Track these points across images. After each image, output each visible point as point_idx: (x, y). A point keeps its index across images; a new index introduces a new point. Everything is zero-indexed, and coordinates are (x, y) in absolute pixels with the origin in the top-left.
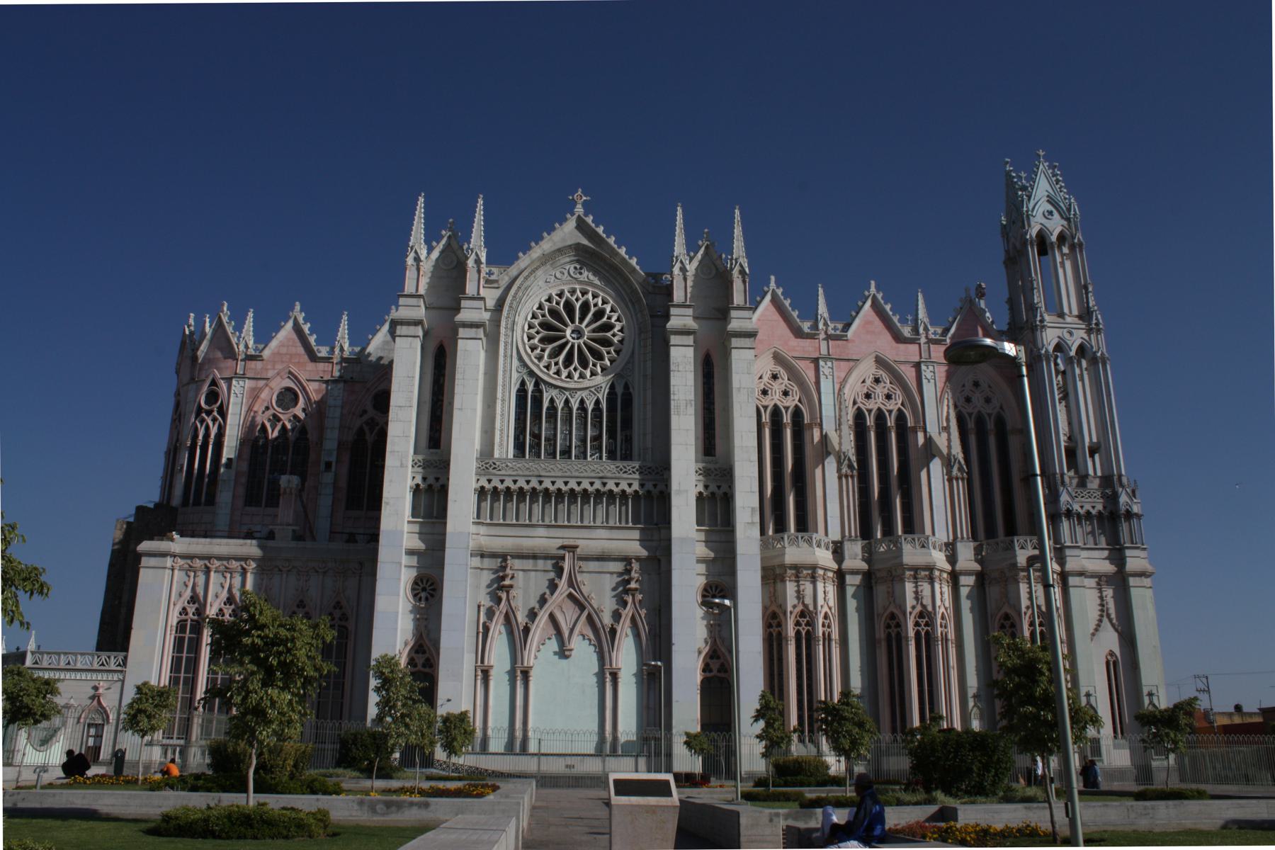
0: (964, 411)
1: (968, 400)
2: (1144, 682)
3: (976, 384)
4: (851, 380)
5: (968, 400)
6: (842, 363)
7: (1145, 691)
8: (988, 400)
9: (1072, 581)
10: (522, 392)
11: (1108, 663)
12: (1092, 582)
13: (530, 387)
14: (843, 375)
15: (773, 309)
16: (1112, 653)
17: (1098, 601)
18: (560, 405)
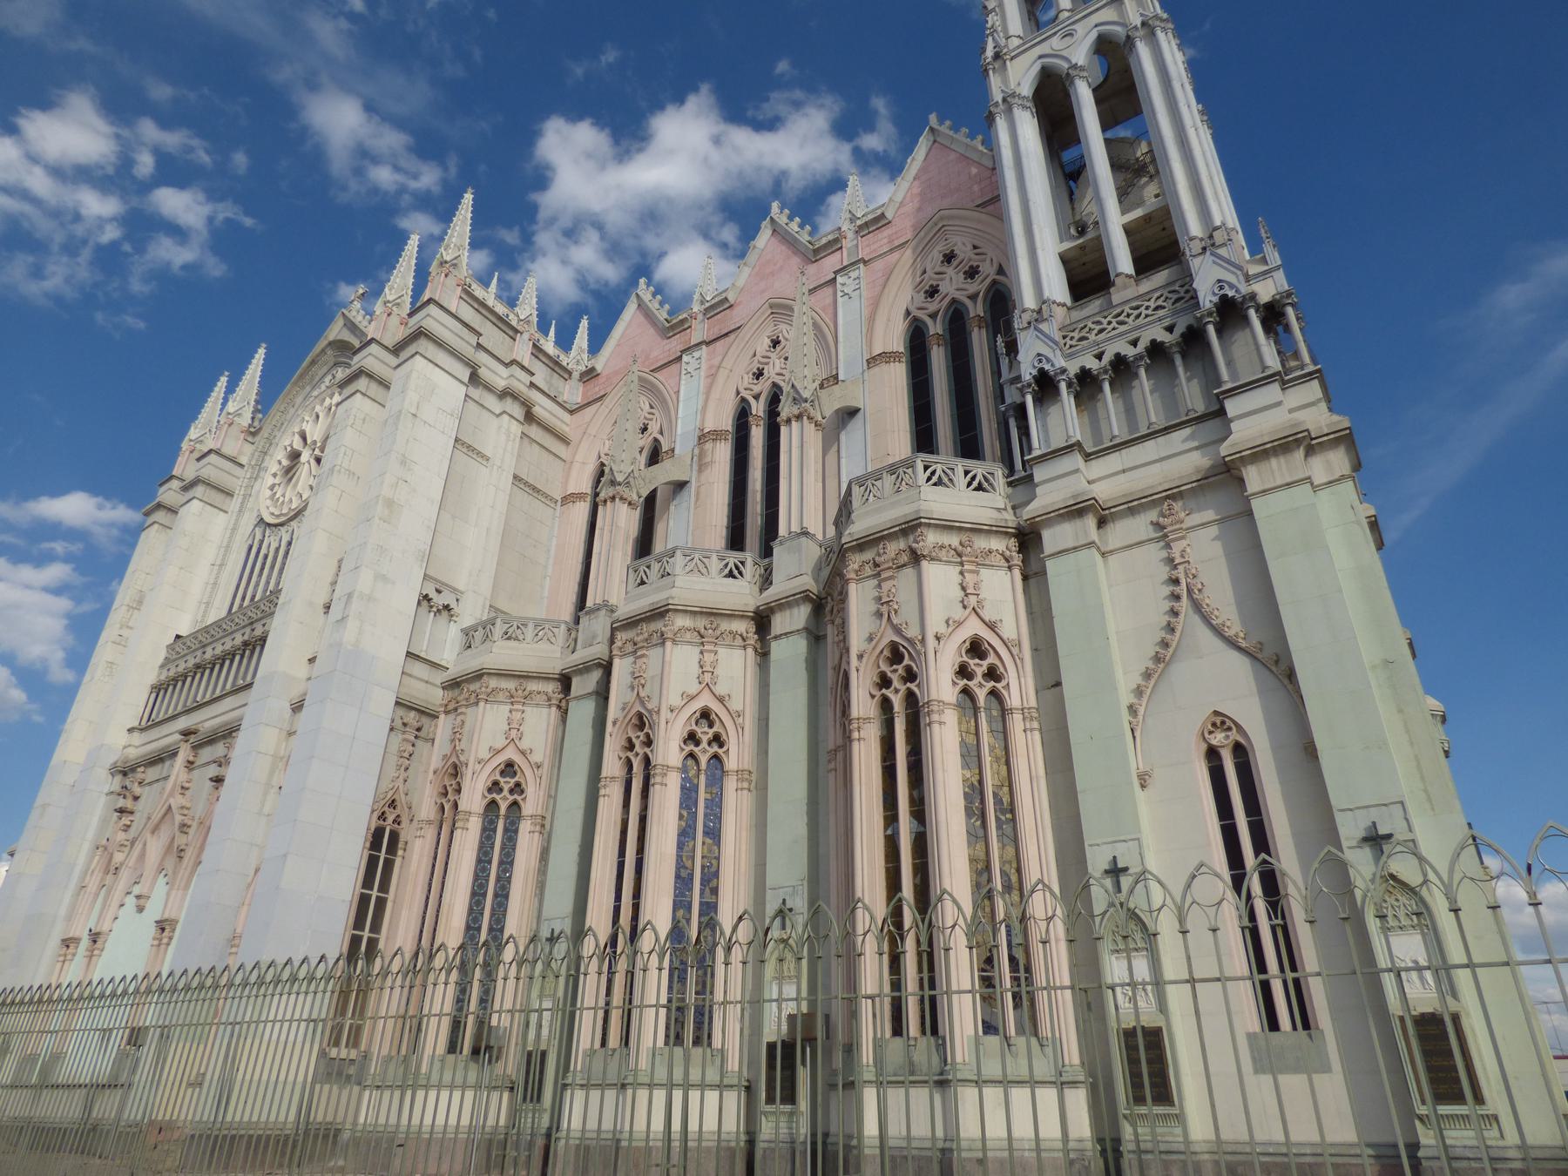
0: (920, 314)
1: (932, 292)
2: (1337, 798)
3: (949, 258)
4: (728, 363)
5: (932, 292)
6: (718, 344)
7: (1350, 829)
8: (972, 273)
9: (1053, 538)
10: (250, 548)
11: (1212, 754)
12: (1139, 526)
13: (258, 537)
14: (716, 362)
15: (641, 318)
16: (1221, 721)
17: (1164, 572)
18: (274, 546)
